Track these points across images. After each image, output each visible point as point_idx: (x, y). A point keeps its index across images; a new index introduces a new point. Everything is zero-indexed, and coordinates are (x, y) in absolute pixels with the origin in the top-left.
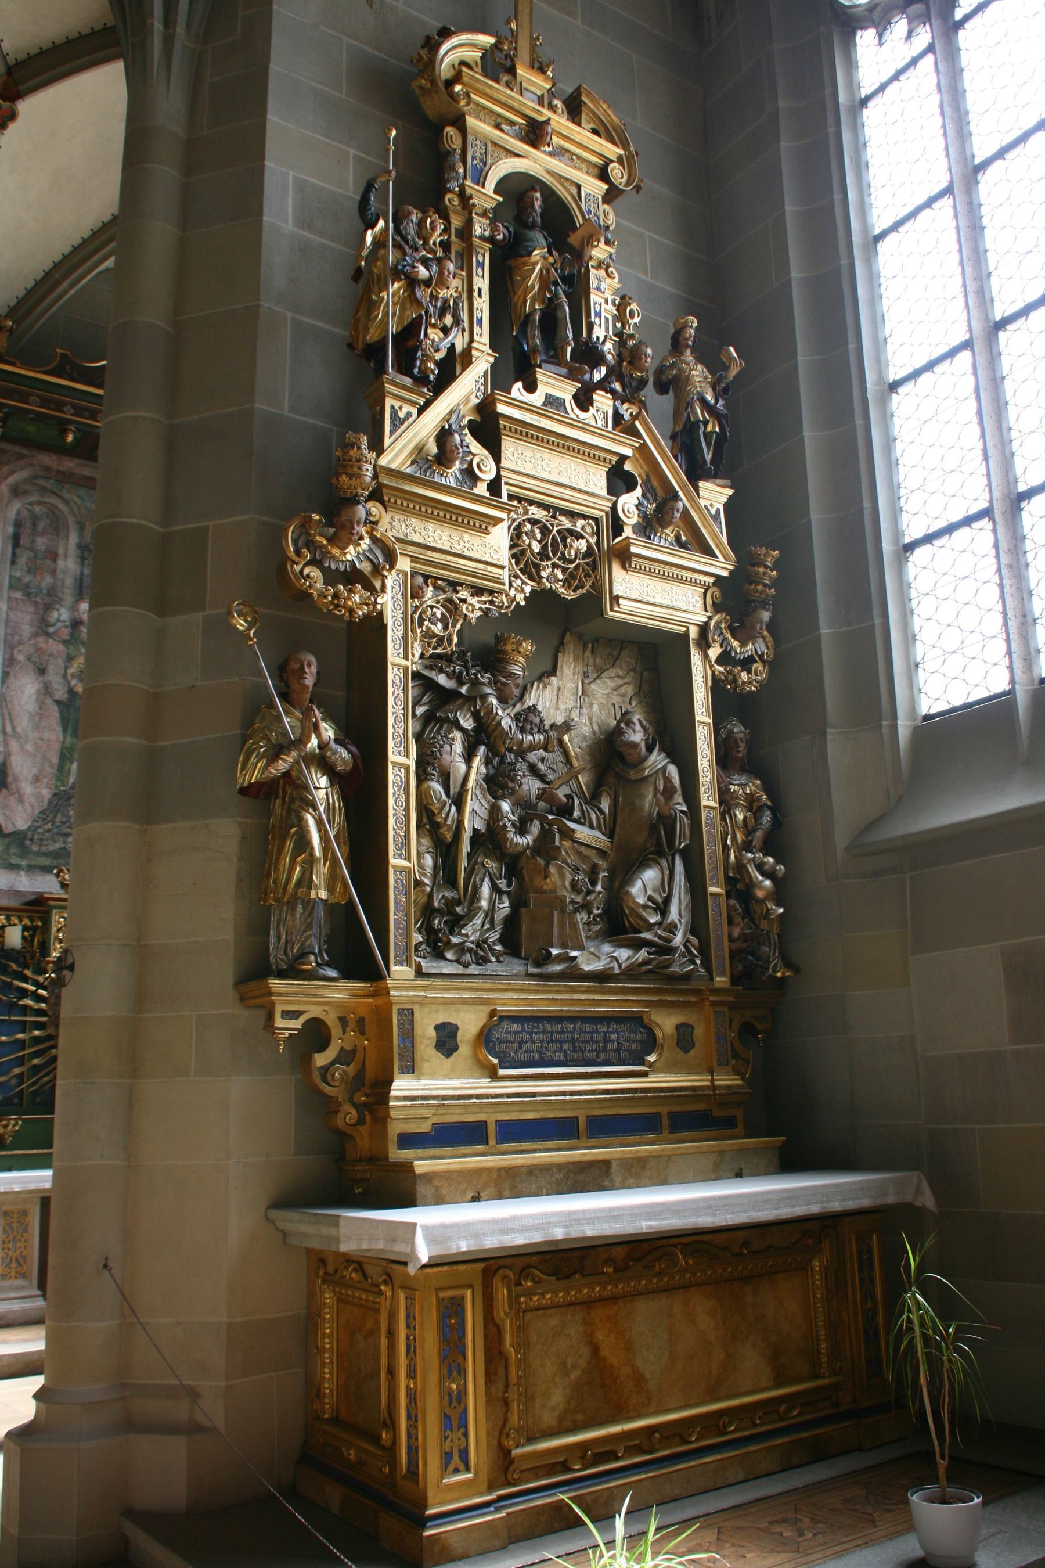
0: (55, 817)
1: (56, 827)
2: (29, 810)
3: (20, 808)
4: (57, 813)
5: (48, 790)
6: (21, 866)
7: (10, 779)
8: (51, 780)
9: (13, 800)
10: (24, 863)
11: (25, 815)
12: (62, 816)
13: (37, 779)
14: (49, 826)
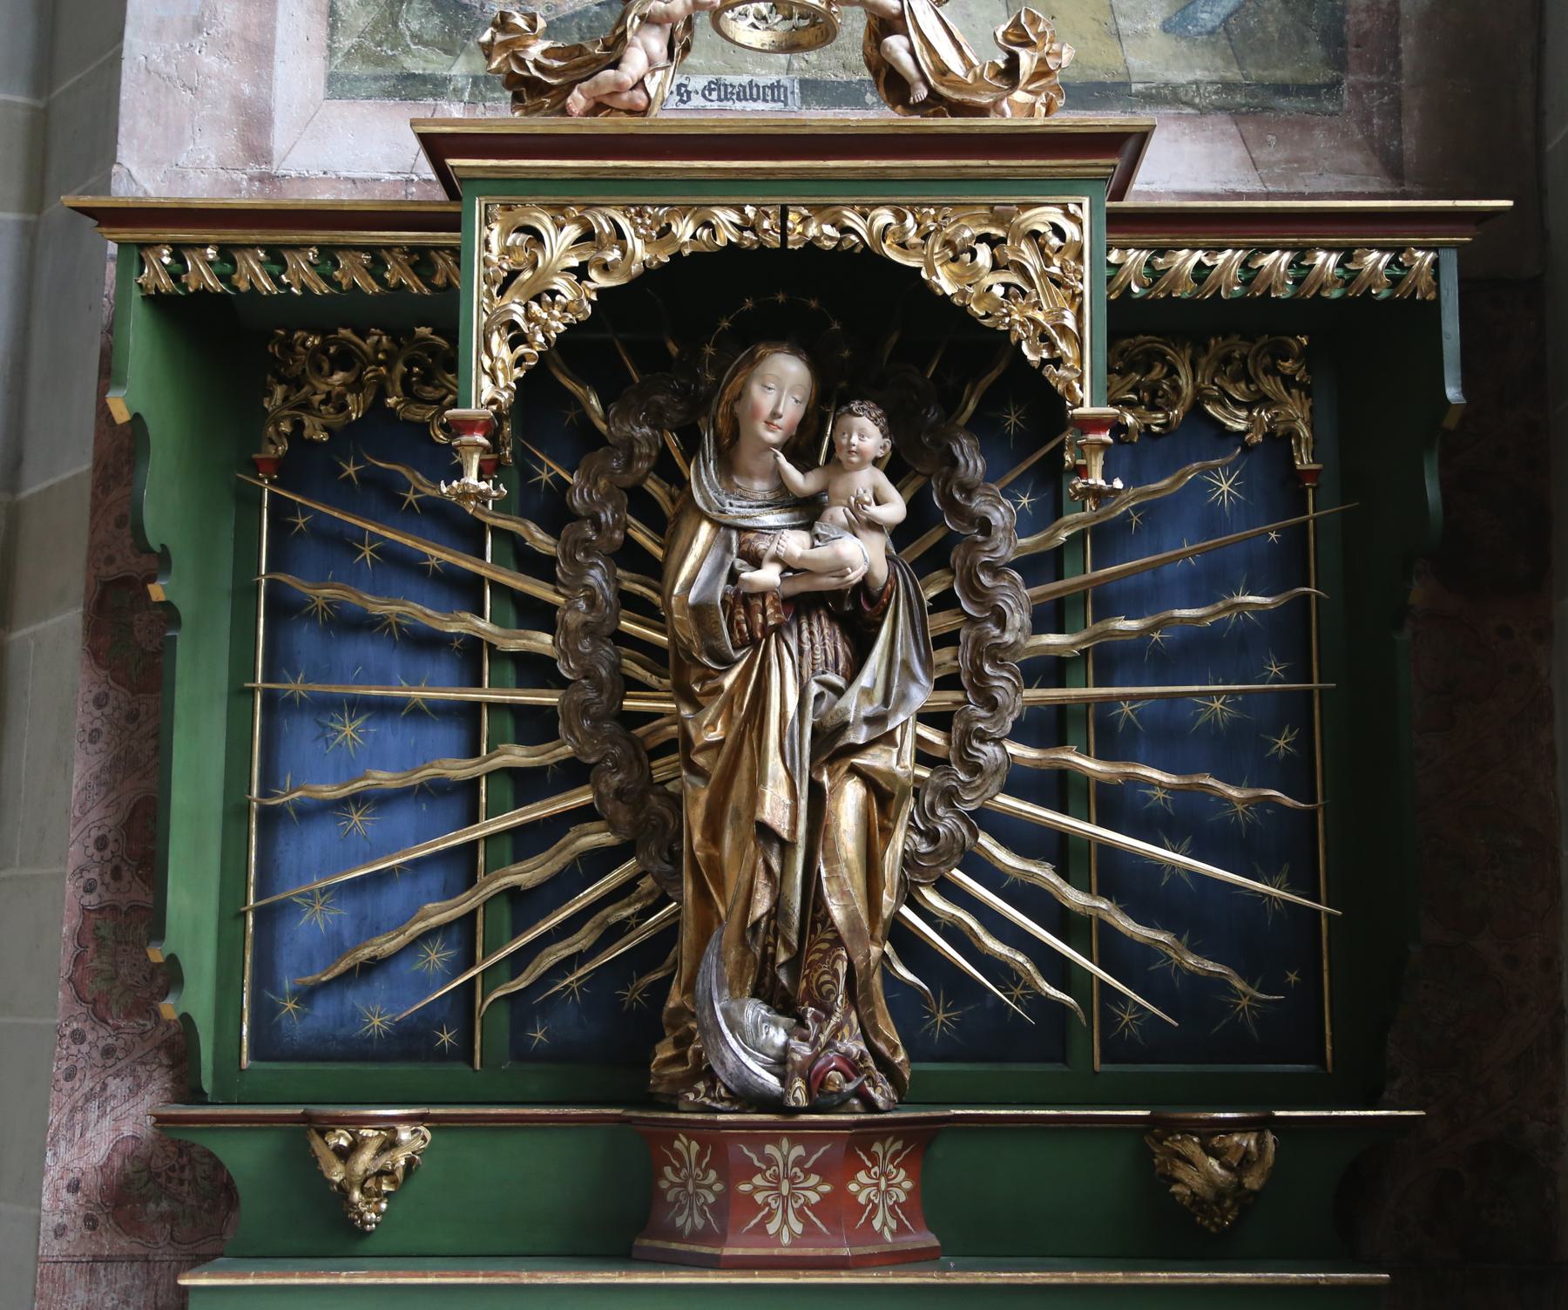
6: (446, 80)
10: (460, 69)
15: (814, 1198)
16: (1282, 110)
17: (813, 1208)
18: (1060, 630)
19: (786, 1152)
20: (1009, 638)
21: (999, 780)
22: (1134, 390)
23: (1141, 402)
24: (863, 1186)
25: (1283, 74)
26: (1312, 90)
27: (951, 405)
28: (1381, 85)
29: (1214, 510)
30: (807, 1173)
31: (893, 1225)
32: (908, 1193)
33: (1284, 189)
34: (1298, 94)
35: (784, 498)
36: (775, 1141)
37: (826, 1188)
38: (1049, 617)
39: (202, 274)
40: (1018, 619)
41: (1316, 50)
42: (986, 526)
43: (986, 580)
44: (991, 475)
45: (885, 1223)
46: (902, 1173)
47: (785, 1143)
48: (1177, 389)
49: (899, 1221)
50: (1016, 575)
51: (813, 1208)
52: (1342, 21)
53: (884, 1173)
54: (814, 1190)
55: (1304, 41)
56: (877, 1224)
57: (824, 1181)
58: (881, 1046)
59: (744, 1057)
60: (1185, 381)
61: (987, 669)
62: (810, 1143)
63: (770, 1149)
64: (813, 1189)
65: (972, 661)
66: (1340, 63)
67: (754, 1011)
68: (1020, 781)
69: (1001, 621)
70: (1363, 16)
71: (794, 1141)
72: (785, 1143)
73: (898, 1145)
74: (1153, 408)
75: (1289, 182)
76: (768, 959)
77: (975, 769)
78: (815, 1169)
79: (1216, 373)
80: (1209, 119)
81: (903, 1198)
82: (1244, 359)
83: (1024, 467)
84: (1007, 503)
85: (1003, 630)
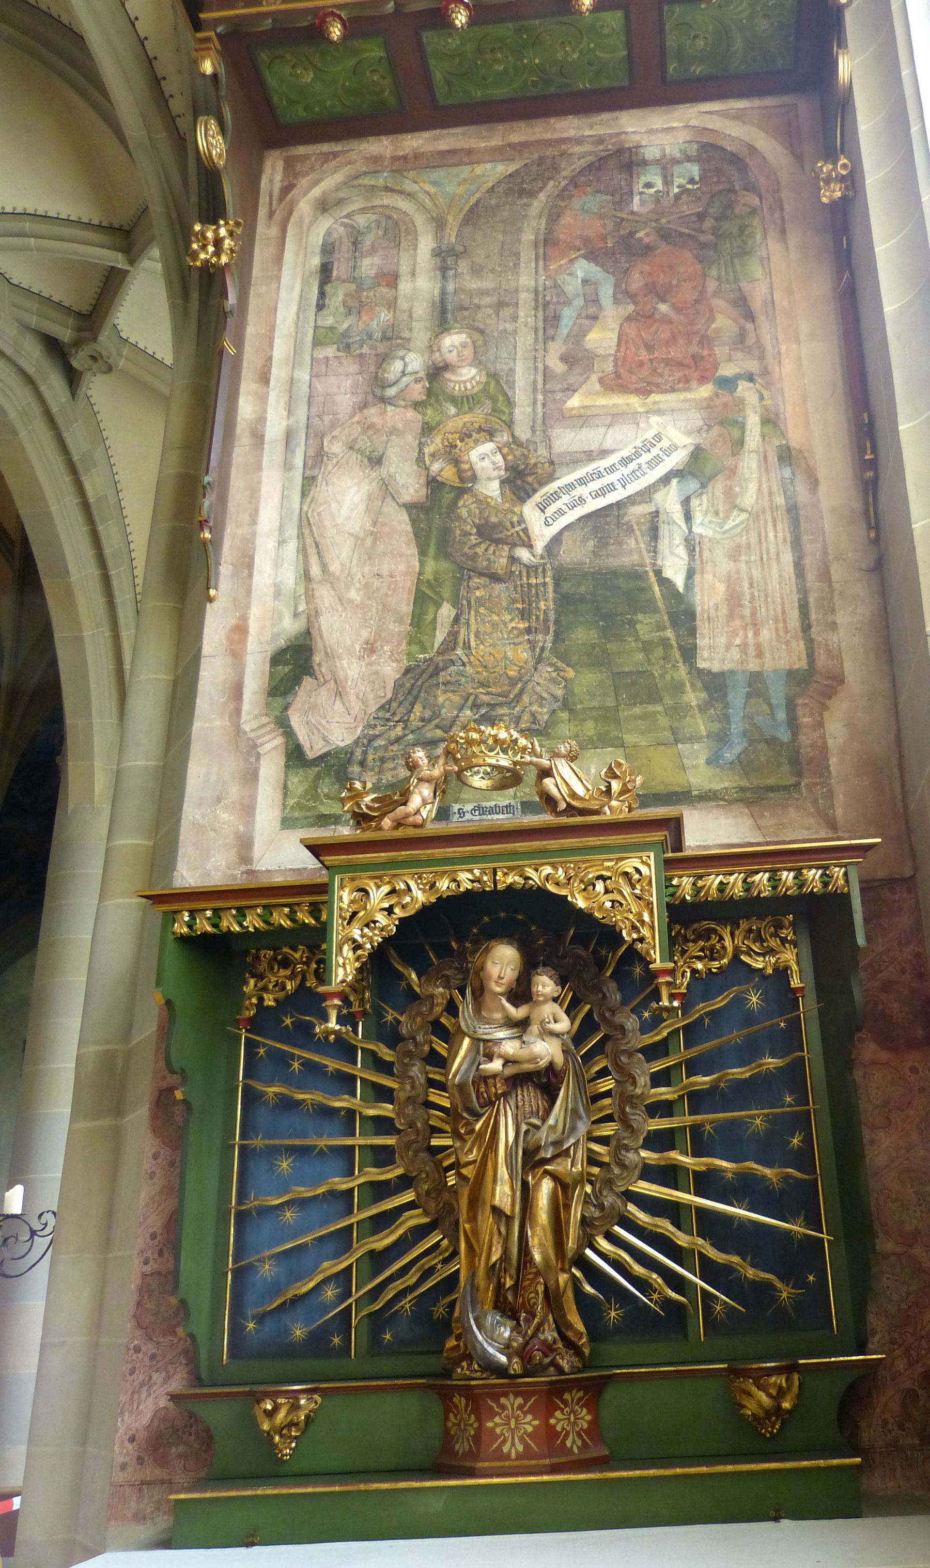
0: (410, 712)
1: (413, 732)
2: (356, 707)
3: (338, 706)
4: (413, 705)
5: (394, 665)
7: (317, 658)
8: (400, 644)
9: (324, 695)
11: (349, 719)
12: (424, 708)
13: (370, 648)
14: (399, 730)
15: (530, 1429)
16: (771, 799)
17: (529, 1435)
18: (668, 1085)
19: (513, 1402)
20: (638, 1091)
21: (637, 1172)
22: (702, 950)
23: (706, 956)
24: (559, 1420)
25: (770, 781)
26: (786, 788)
27: (601, 964)
28: (822, 783)
29: (750, 1012)
30: (525, 1414)
31: (579, 1443)
32: (589, 1423)
33: (776, 839)
34: (779, 790)
35: (510, 1023)
36: (506, 1395)
37: (536, 1423)
38: (659, 1079)
39: (204, 925)
40: (643, 1080)
41: (786, 768)
42: (622, 1028)
43: (624, 1059)
44: (624, 1002)
45: (574, 1442)
46: (585, 1410)
47: (511, 1397)
48: (724, 948)
49: (584, 1442)
50: (640, 1055)
51: (529, 1435)
52: (798, 752)
53: (572, 1411)
54: (529, 1423)
55: (780, 764)
56: (568, 1443)
57: (535, 1419)
58: (570, 1334)
59: (486, 1345)
60: (728, 943)
61: (628, 1109)
62: (526, 1396)
63: (503, 1400)
64: (529, 1423)
65: (619, 1105)
66: (800, 774)
67: (491, 1318)
68: (649, 1173)
69: (634, 1083)
70: (809, 750)
71: (516, 1395)
72: (511, 1397)
73: (581, 1394)
74: (713, 959)
75: (778, 836)
76: (500, 1286)
77: (623, 1166)
78: (528, 1412)
79: (745, 938)
80: (733, 806)
81: (585, 1426)
82: (759, 930)
83: (642, 996)
84: (634, 1016)
85: (635, 1088)
